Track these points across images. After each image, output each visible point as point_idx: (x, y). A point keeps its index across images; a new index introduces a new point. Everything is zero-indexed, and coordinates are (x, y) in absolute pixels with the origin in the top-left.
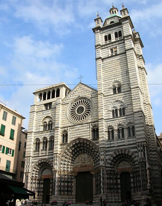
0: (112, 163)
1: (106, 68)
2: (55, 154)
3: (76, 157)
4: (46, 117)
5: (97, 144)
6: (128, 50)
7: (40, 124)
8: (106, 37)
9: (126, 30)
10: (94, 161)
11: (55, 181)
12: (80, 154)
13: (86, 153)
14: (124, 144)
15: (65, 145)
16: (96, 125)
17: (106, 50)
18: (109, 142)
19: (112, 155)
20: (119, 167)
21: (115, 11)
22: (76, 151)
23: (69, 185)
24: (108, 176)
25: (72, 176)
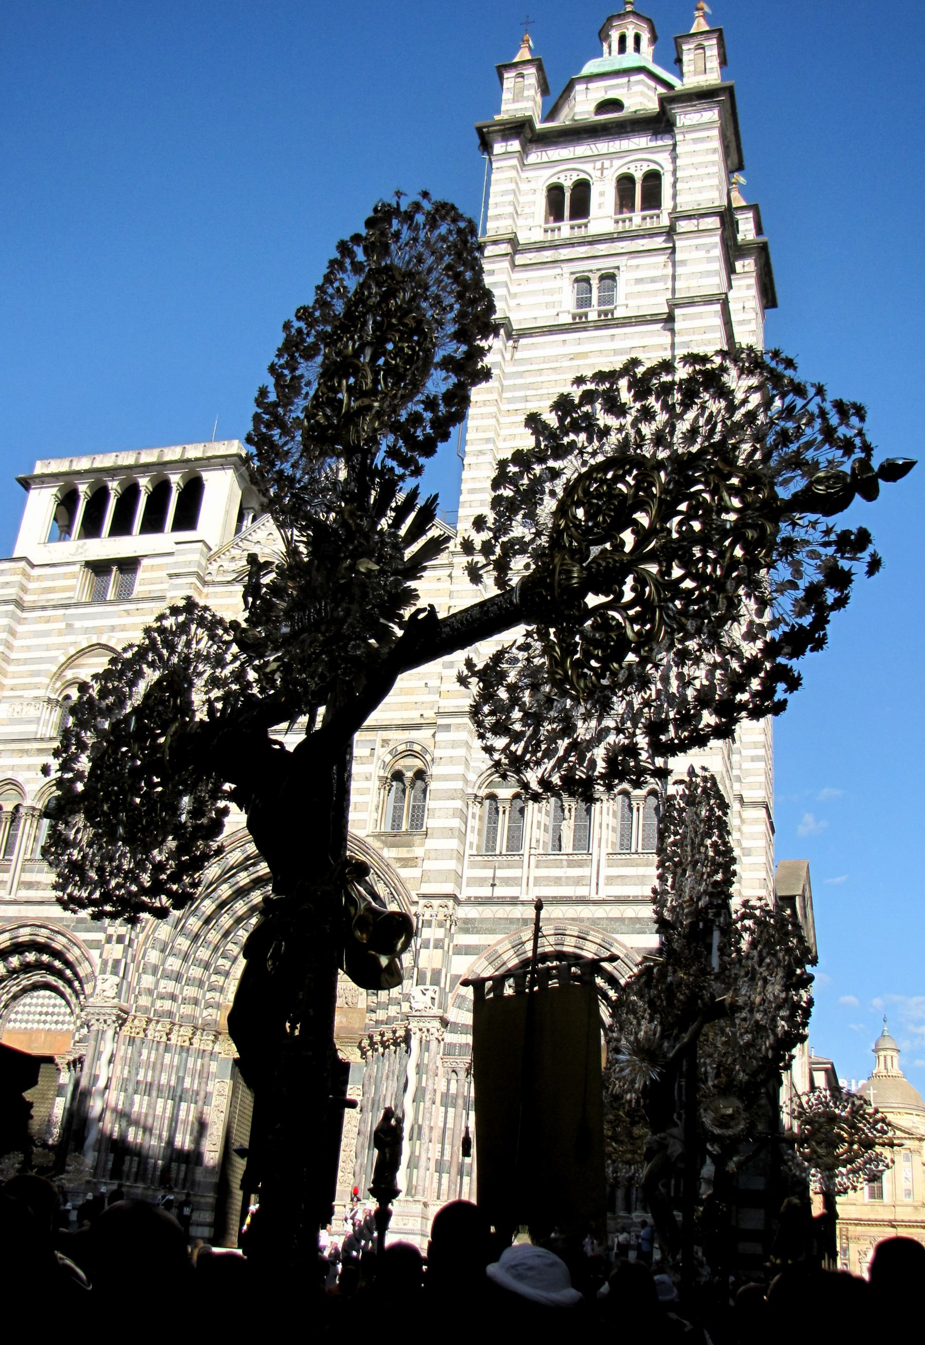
1: (529, 393)
4: (82, 652)
5: (404, 873)
6: (691, 302)
7: (37, 687)
8: (555, 192)
9: (693, 172)
14: (582, 891)
16: (417, 748)
17: (542, 280)
21: (637, 38)
23: (182, 1115)
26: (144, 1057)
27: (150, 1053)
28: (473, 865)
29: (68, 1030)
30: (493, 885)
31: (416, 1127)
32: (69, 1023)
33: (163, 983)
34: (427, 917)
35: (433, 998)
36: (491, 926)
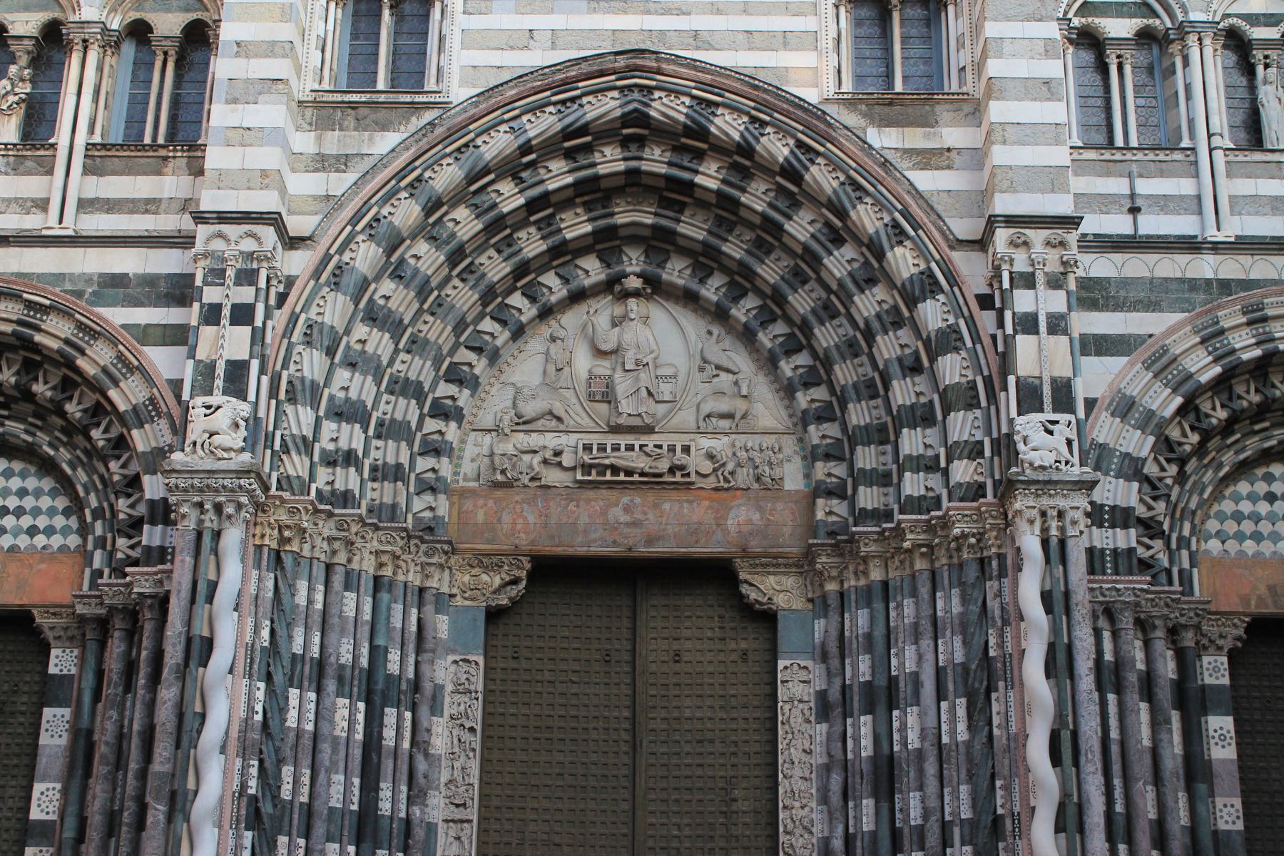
0: (1151, 469)
2: (223, 217)
3: (519, 332)
5: (925, 180)
10: (824, 415)
11: (200, 649)
12: (578, 296)
13: (689, 298)
15: (384, 127)
18: (1108, 169)
19: (1162, 364)
20: (1222, 536)
22: (532, 244)
23: (389, 734)
24: (1106, 635)
25: (442, 602)
26: (301, 599)
27: (311, 589)
28: (1080, 167)
29: (63, 549)
30: (1134, 210)
31: (1066, 735)
32: (65, 531)
33: (329, 427)
34: (1021, 265)
35: (1069, 443)
36: (1153, 296)
